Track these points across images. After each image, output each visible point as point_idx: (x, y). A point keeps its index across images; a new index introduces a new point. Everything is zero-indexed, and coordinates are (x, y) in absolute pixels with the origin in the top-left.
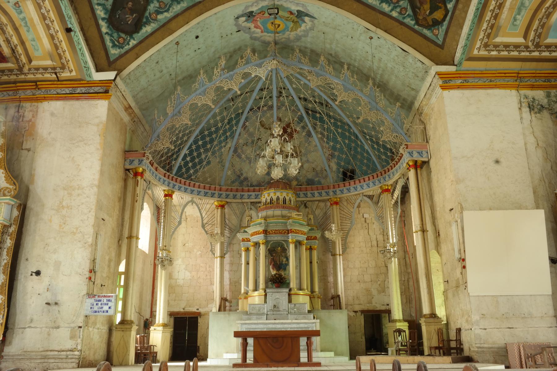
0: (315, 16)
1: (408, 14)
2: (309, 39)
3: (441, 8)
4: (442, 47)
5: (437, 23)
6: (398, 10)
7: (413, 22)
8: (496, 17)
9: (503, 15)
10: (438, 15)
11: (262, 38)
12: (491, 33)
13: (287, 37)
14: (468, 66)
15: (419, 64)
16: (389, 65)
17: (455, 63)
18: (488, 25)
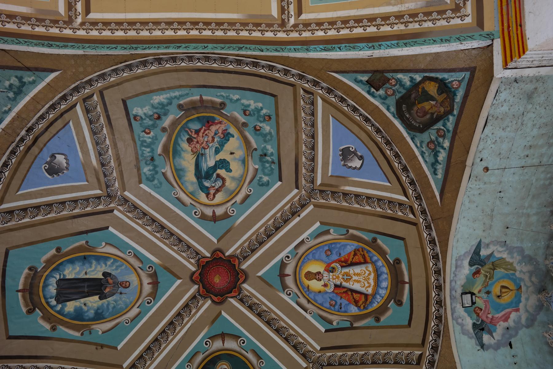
0: (475, 243)
1: (443, 126)
2: (527, 246)
3: (423, 88)
4: (472, 70)
5: (444, 87)
6: (441, 140)
7: (451, 118)
8: (413, 15)
9: (410, 7)
10: (432, 89)
11: (530, 310)
12: (436, 12)
13: (527, 274)
14: (492, 22)
15: (503, 96)
16: (535, 132)
17: (491, 43)
18: (425, 21)
